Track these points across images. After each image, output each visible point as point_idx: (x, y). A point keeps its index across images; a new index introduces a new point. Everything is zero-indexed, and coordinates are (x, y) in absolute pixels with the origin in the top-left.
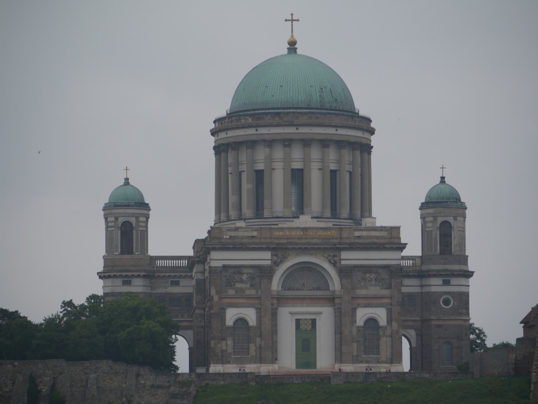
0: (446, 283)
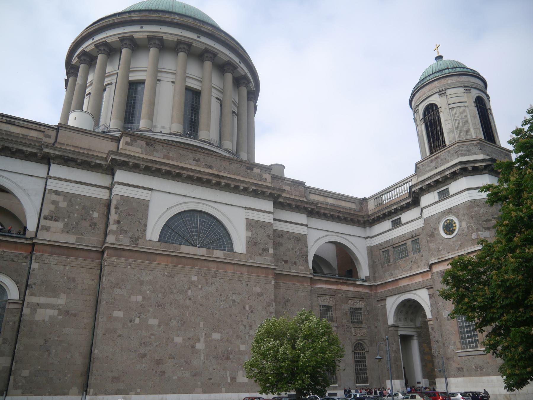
0: (444, 195)
